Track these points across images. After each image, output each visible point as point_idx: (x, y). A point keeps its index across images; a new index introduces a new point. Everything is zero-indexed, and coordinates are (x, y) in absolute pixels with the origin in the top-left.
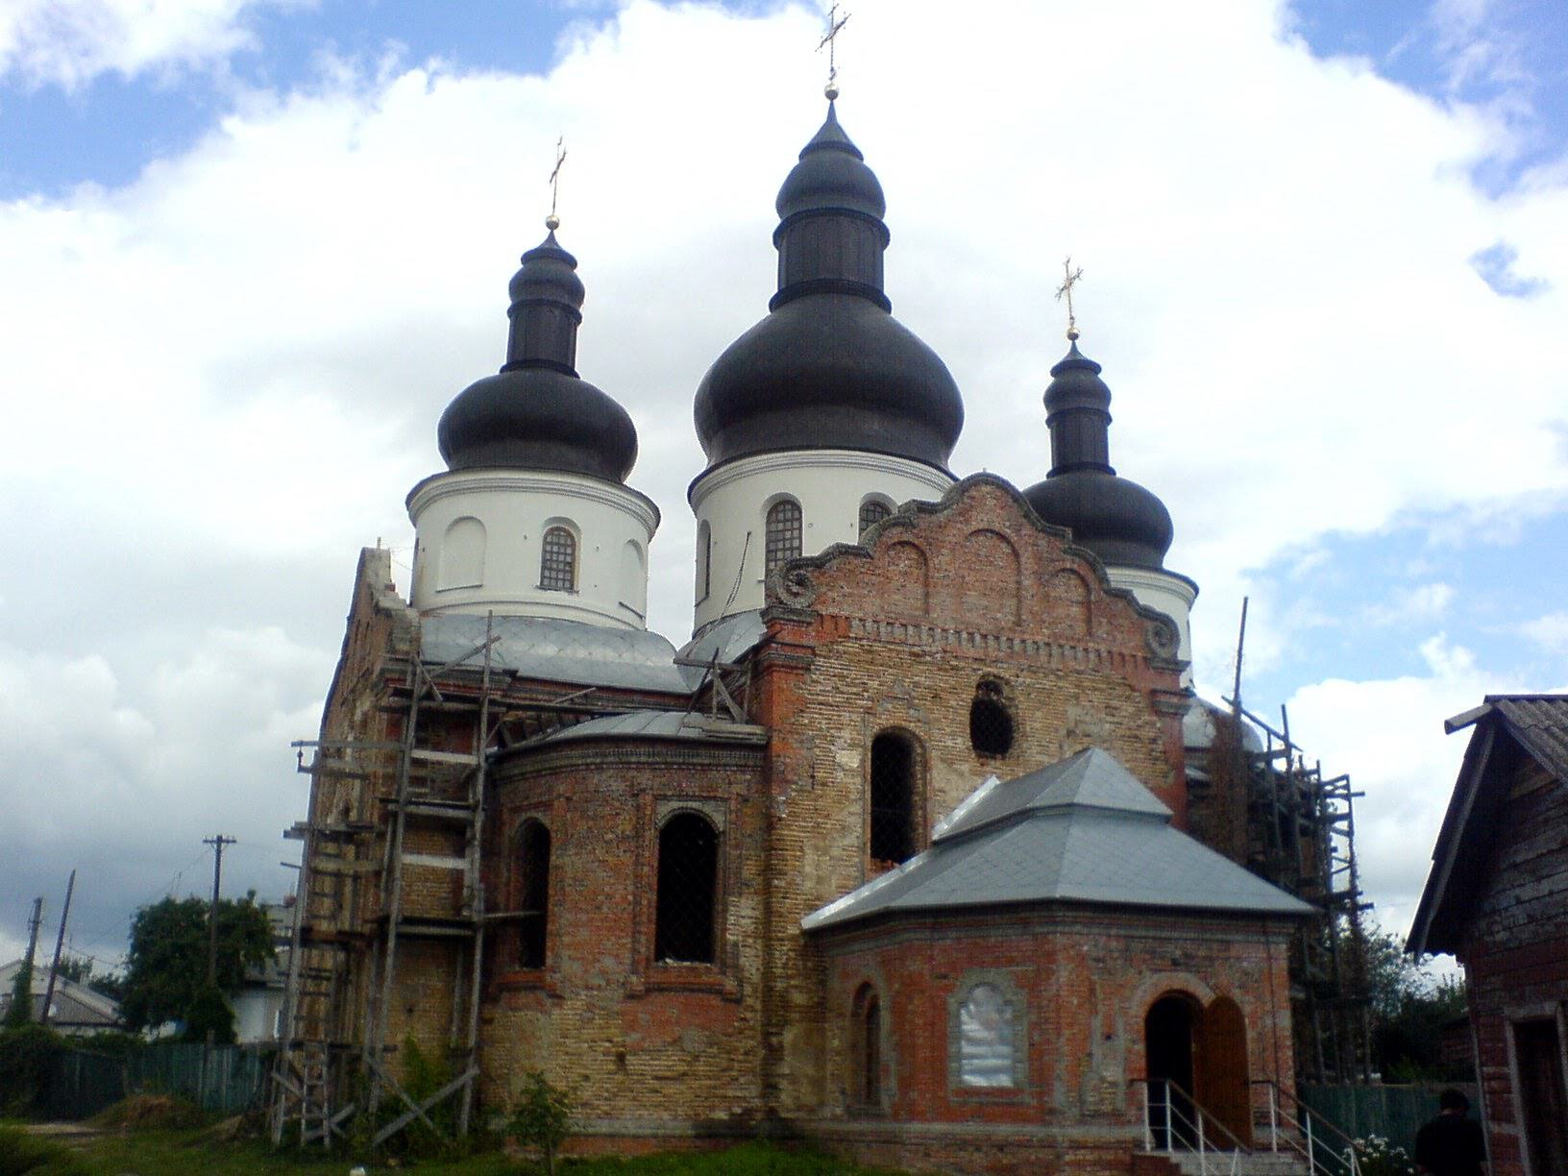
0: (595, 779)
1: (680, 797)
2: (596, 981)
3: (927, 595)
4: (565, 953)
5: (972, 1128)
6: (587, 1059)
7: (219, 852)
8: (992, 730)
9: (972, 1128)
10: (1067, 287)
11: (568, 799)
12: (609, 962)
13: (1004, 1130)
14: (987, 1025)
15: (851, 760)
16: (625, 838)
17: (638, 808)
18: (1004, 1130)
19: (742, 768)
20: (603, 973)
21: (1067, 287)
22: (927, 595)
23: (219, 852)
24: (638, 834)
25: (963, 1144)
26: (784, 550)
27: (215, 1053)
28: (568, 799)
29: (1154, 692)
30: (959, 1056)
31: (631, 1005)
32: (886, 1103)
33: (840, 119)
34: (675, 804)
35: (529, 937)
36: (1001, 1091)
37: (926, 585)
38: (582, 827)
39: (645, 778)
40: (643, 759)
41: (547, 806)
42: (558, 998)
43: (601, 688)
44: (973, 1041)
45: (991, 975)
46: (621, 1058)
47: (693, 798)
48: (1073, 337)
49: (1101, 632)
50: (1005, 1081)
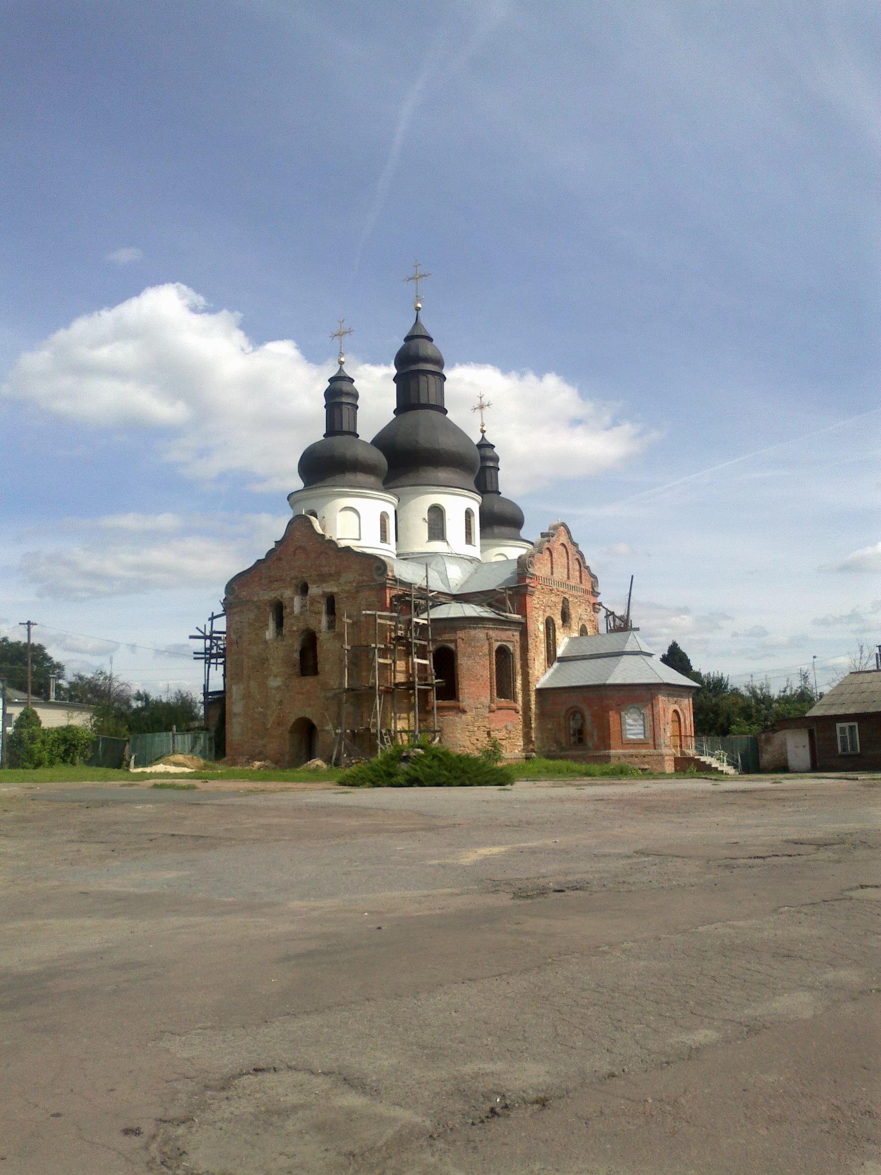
0: (473, 632)
1: (500, 641)
2: (479, 706)
3: (552, 568)
4: (466, 696)
5: (632, 751)
6: (477, 734)
7: (29, 630)
8: (565, 616)
9: (632, 751)
10: (481, 407)
12: (483, 699)
13: (644, 751)
14: (635, 720)
15: (542, 627)
16: (485, 655)
17: (490, 644)
18: (644, 751)
19: (516, 630)
20: (481, 703)
21: (481, 407)
22: (552, 568)
23: (29, 630)
24: (490, 654)
25: (632, 756)
27: (179, 737)
29: (594, 604)
30: (626, 730)
31: (492, 714)
32: (590, 744)
33: (423, 320)
34: (499, 643)
35: (449, 690)
36: (641, 739)
37: (552, 564)
38: (469, 650)
39: (491, 632)
41: (455, 641)
42: (464, 711)
43: (439, 593)
44: (632, 725)
45: (636, 706)
46: (489, 734)
47: (504, 641)
48: (483, 432)
49: (583, 581)
50: (642, 737)
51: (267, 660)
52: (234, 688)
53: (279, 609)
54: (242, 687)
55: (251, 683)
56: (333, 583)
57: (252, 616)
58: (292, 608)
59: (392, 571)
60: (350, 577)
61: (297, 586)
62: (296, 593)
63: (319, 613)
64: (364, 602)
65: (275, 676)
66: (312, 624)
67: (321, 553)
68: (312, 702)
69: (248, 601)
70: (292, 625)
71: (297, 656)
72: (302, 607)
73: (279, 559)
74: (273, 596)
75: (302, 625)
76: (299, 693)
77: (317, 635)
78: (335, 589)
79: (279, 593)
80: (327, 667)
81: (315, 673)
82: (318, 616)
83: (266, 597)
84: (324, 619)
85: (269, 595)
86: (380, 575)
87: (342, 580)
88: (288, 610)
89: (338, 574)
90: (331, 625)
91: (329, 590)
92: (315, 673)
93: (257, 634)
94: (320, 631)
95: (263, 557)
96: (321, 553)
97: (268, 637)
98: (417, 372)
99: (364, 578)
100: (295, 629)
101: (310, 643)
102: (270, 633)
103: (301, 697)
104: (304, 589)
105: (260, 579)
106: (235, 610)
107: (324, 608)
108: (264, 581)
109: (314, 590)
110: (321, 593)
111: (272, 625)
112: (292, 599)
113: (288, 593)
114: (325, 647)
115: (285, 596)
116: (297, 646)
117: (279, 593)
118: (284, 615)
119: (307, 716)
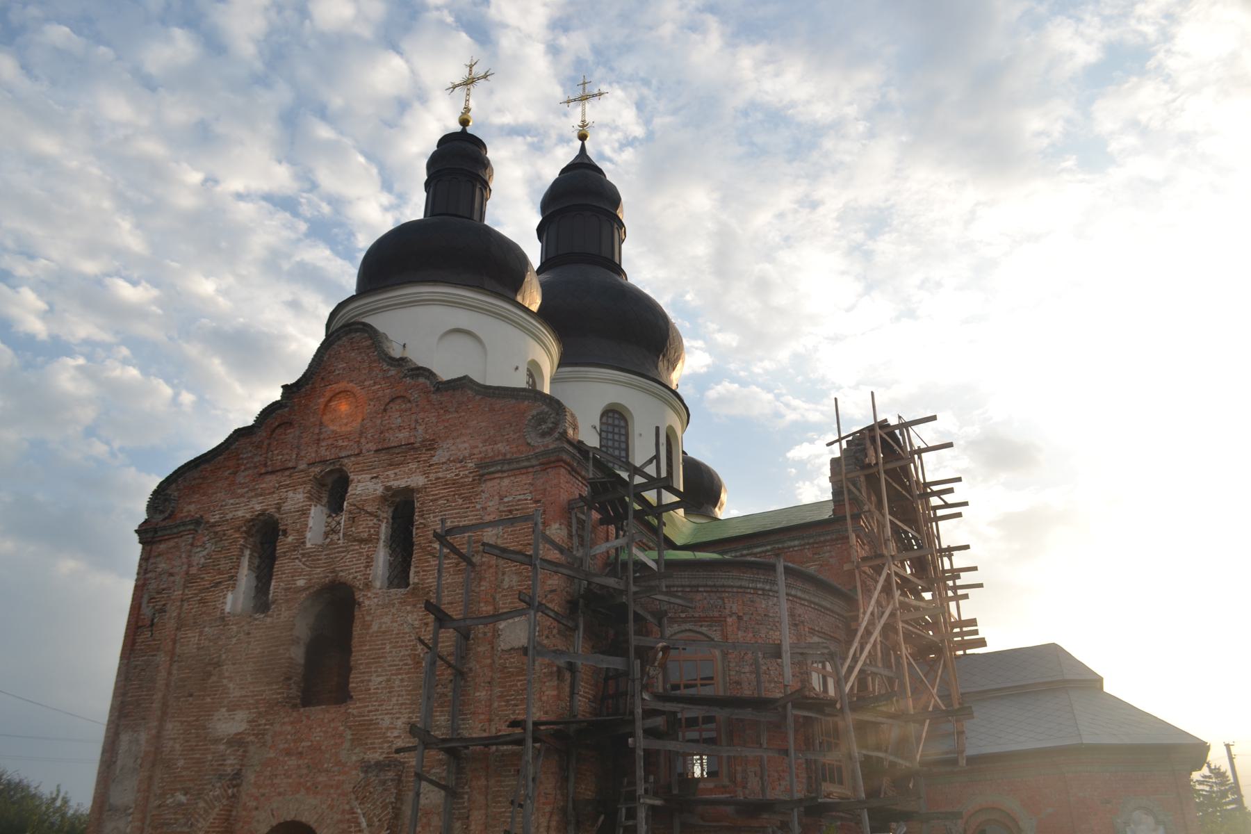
11: (740, 618)
26: (615, 448)
28: (740, 618)
39: (799, 610)
40: (799, 594)
41: (720, 621)
51: (218, 664)
52: (125, 738)
53: (266, 536)
54: (143, 736)
55: (169, 726)
56: (413, 466)
57: (199, 558)
58: (301, 533)
59: (575, 428)
60: (461, 447)
61: (320, 482)
62: (313, 498)
63: (370, 540)
64: (493, 505)
65: (232, 708)
66: (350, 568)
67: (393, 400)
68: (322, 778)
69: (198, 522)
70: (296, 575)
71: (298, 654)
72: (326, 535)
73: (289, 424)
74: (258, 507)
75: (320, 574)
76: (288, 753)
77: (359, 596)
78: (418, 481)
79: (273, 499)
80: (376, 680)
81: (342, 695)
82: (365, 548)
83: (240, 513)
84: (382, 556)
85: (245, 508)
86: (543, 435)
87: (440, 456)
88: (290, 539)
89: (430, 445)
90: (399, 575)
91: (395, 484)
92: (342, 695)
93: (203, 602)
94: (368, 586)
95: (250, 421)
96: (393, 400)
97: (228, 608)
98: (583, 204)
99: (501, 447)
100: (301, 583)
101: (338, 605)
102: (236, 600)
103: (292, 762)
104: (334, 489)
105: (235, 473)
106: (163, 547)
107: (384, 529)
108: (240, 478)
109: (364, 487)
110: (380, 490)
111: (245, 577)
112: (304, 513)
113: (296, 498)
114: (375, 627)
115: (287, 507)
116: (302, 630)
117: (273, 499)
118: (280, 550)
119: (307, 818)
